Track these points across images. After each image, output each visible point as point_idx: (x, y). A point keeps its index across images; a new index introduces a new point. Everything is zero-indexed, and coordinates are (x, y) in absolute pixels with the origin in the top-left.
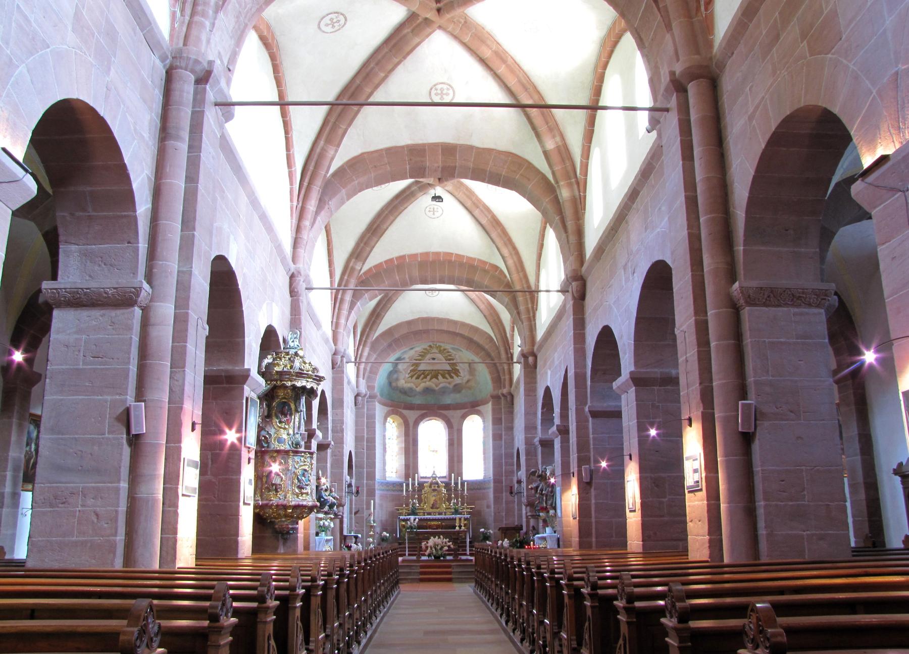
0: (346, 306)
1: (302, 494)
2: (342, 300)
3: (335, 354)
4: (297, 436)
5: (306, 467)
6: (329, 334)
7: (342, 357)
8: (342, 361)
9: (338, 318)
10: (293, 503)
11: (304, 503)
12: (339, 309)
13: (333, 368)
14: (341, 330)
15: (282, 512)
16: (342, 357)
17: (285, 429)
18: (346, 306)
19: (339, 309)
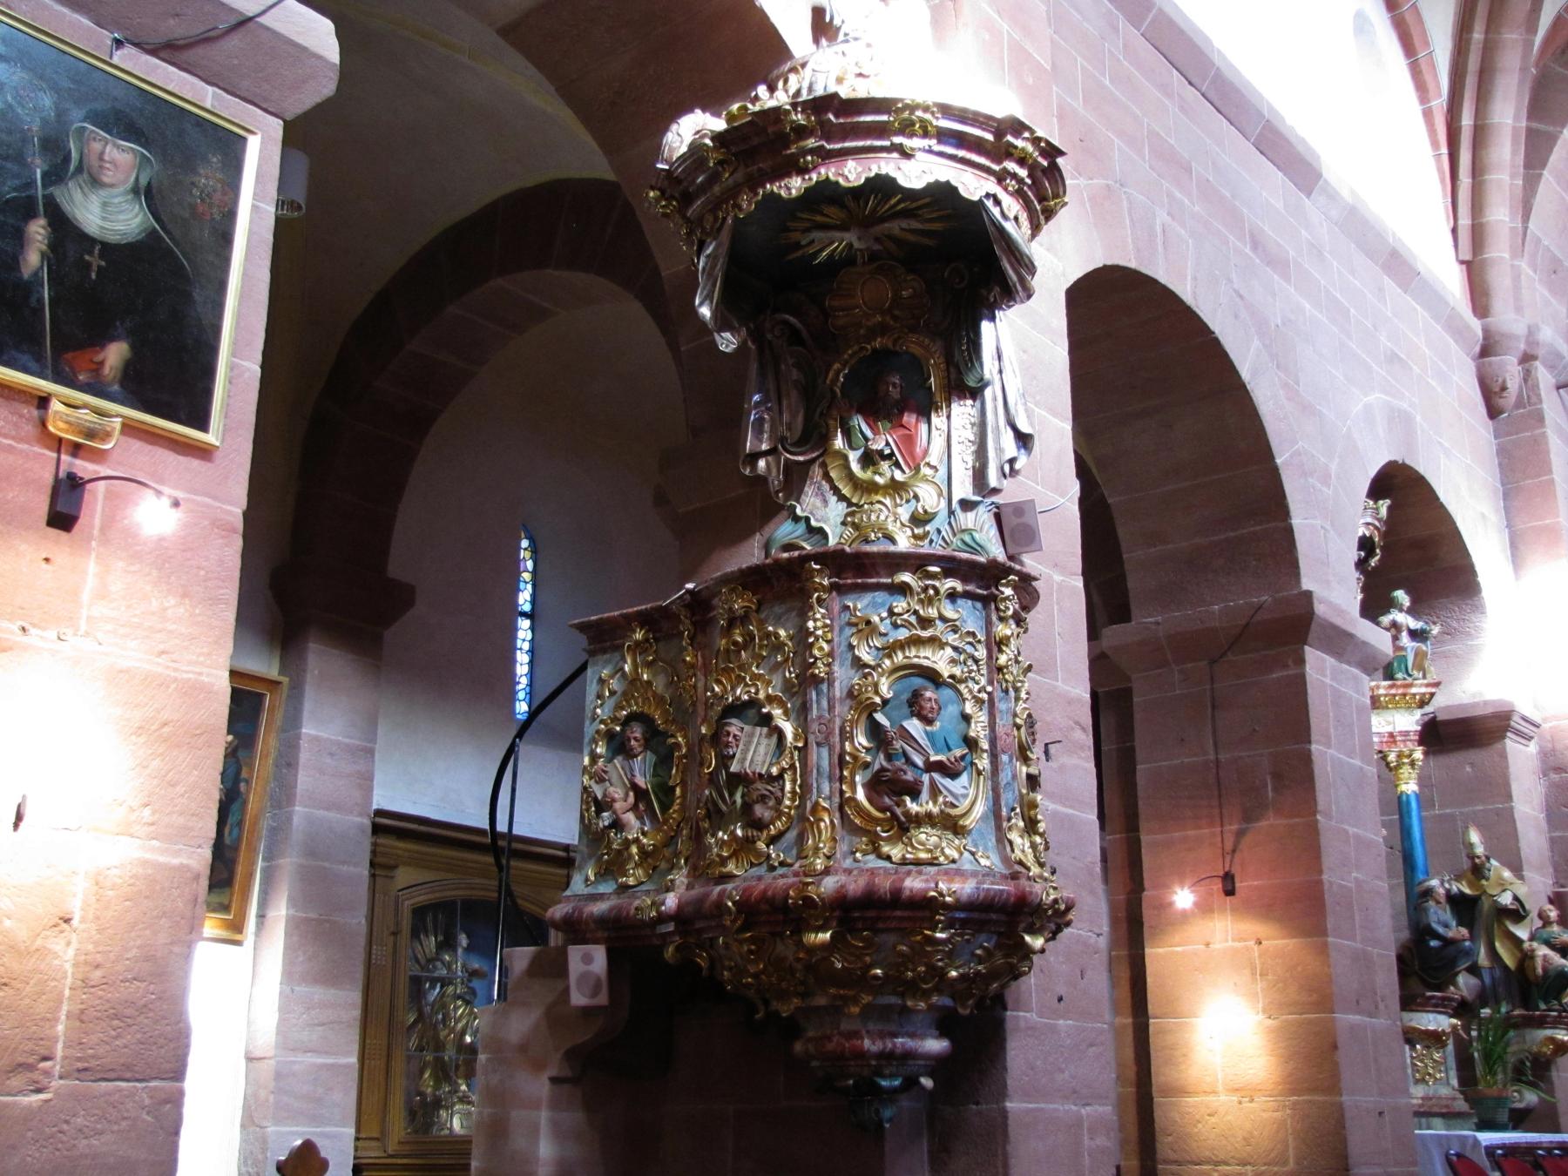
0: (1505, 153)
1: (903, 827)
2: (1481, 134)
3: (1487, 350)
4: (967, 519)
5: (940, 660)
6: (1453, 281)
7: (1527, 359)
8: (1527, 376)
9: (1477, 207)
10: (829, 884)
11: (914, 884)
12: (1477, 171)
13: (1493, 412)
14: (1499, 250)
15: (785, 950)
16: (1527, 359)
17: (895, 488)
18: (1505, 153)
19: (1477, 171)
